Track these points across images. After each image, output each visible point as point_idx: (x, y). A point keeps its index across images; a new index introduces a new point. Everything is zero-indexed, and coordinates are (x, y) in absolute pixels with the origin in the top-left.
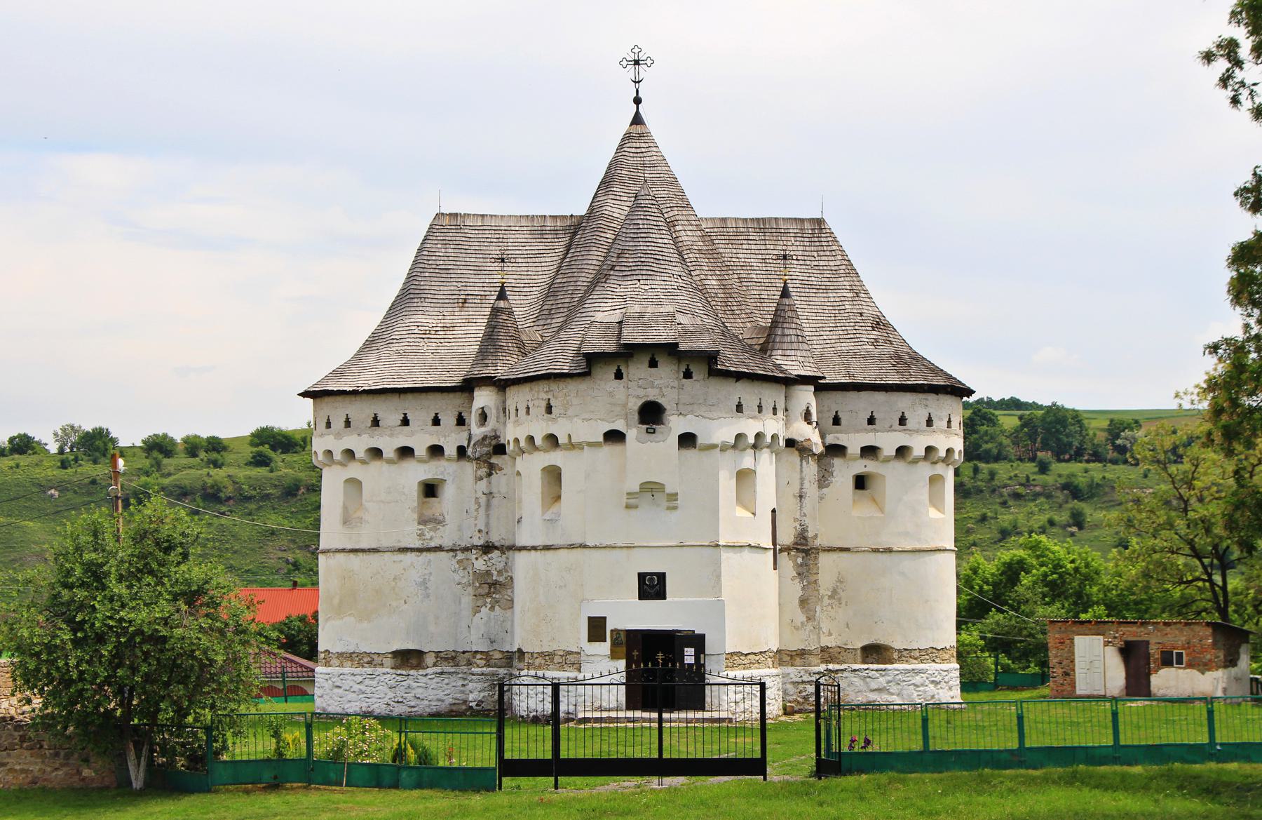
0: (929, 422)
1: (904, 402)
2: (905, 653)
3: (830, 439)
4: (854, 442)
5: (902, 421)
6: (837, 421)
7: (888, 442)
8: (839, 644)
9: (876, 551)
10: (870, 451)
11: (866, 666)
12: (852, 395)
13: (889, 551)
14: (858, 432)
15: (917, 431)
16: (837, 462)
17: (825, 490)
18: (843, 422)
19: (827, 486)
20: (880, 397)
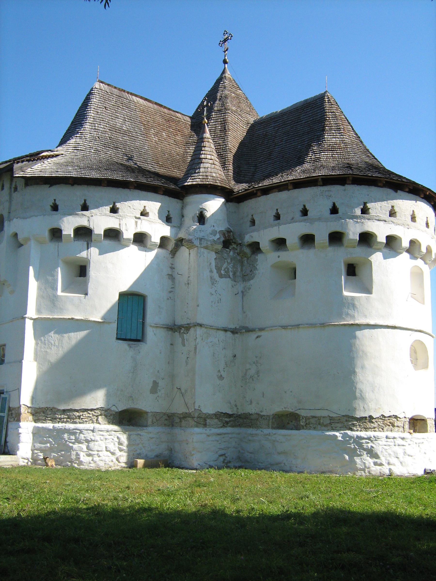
0: (334, 210)
1: (305, 195)
2: (313, 421)
3: (248, 239)
4: (264, 237)
5: (305, 212)
6: (253, 222)
7: (292, 232)
8: (257, 411)
9: (284, 327)
10: (280, 243)
11: (274, 431)
12: (262, 199)
13: (297, 326)
14: (265, 228)
15: (319, 219)
16: (260, 257)
17: (252, 282)
18: (256, 222)
19: (252, 279)
20: (284, 195)
